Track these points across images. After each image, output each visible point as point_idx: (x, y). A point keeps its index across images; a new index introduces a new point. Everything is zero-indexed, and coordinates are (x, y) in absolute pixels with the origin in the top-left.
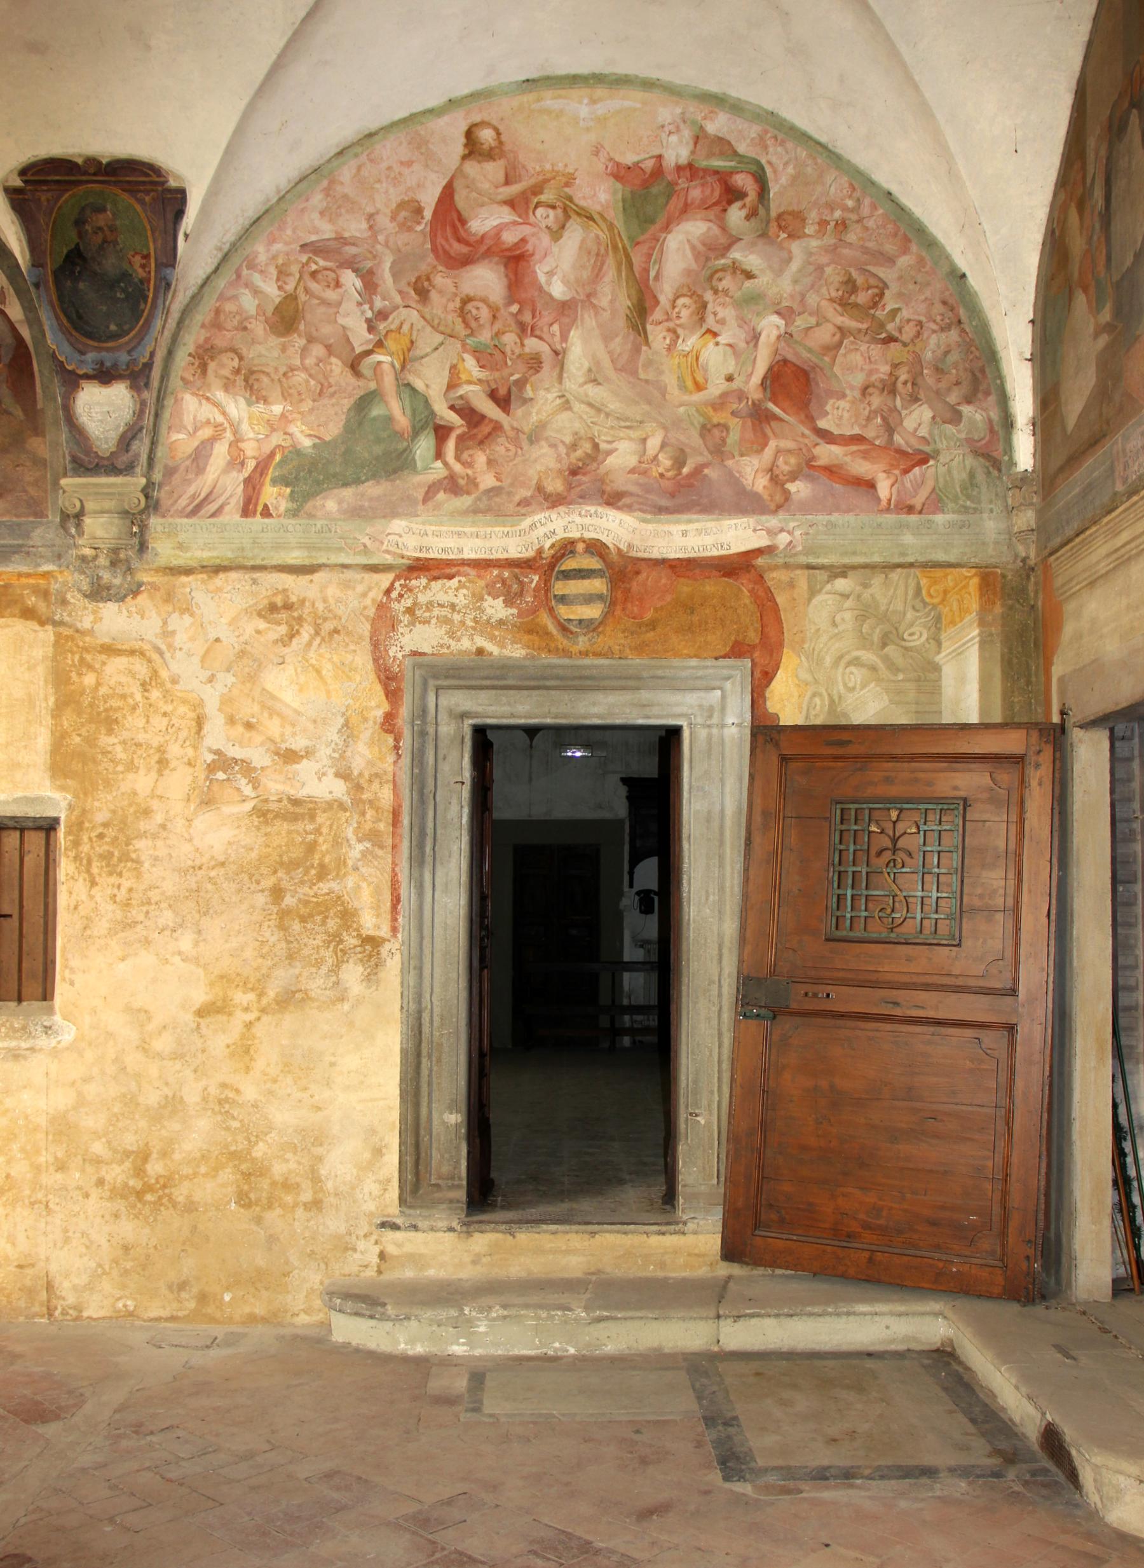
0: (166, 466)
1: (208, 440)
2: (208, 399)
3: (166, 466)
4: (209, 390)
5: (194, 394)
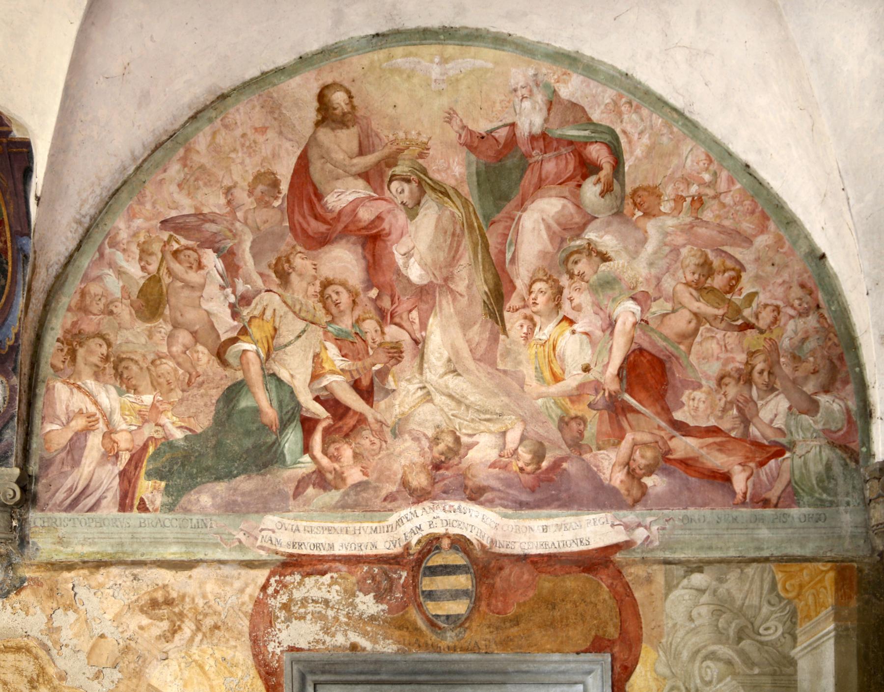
0: (41, 458)
1: (83, 430)
2: (79, 388)
3: (41, 458)
4: (80, 379)
5: (64, 382)
